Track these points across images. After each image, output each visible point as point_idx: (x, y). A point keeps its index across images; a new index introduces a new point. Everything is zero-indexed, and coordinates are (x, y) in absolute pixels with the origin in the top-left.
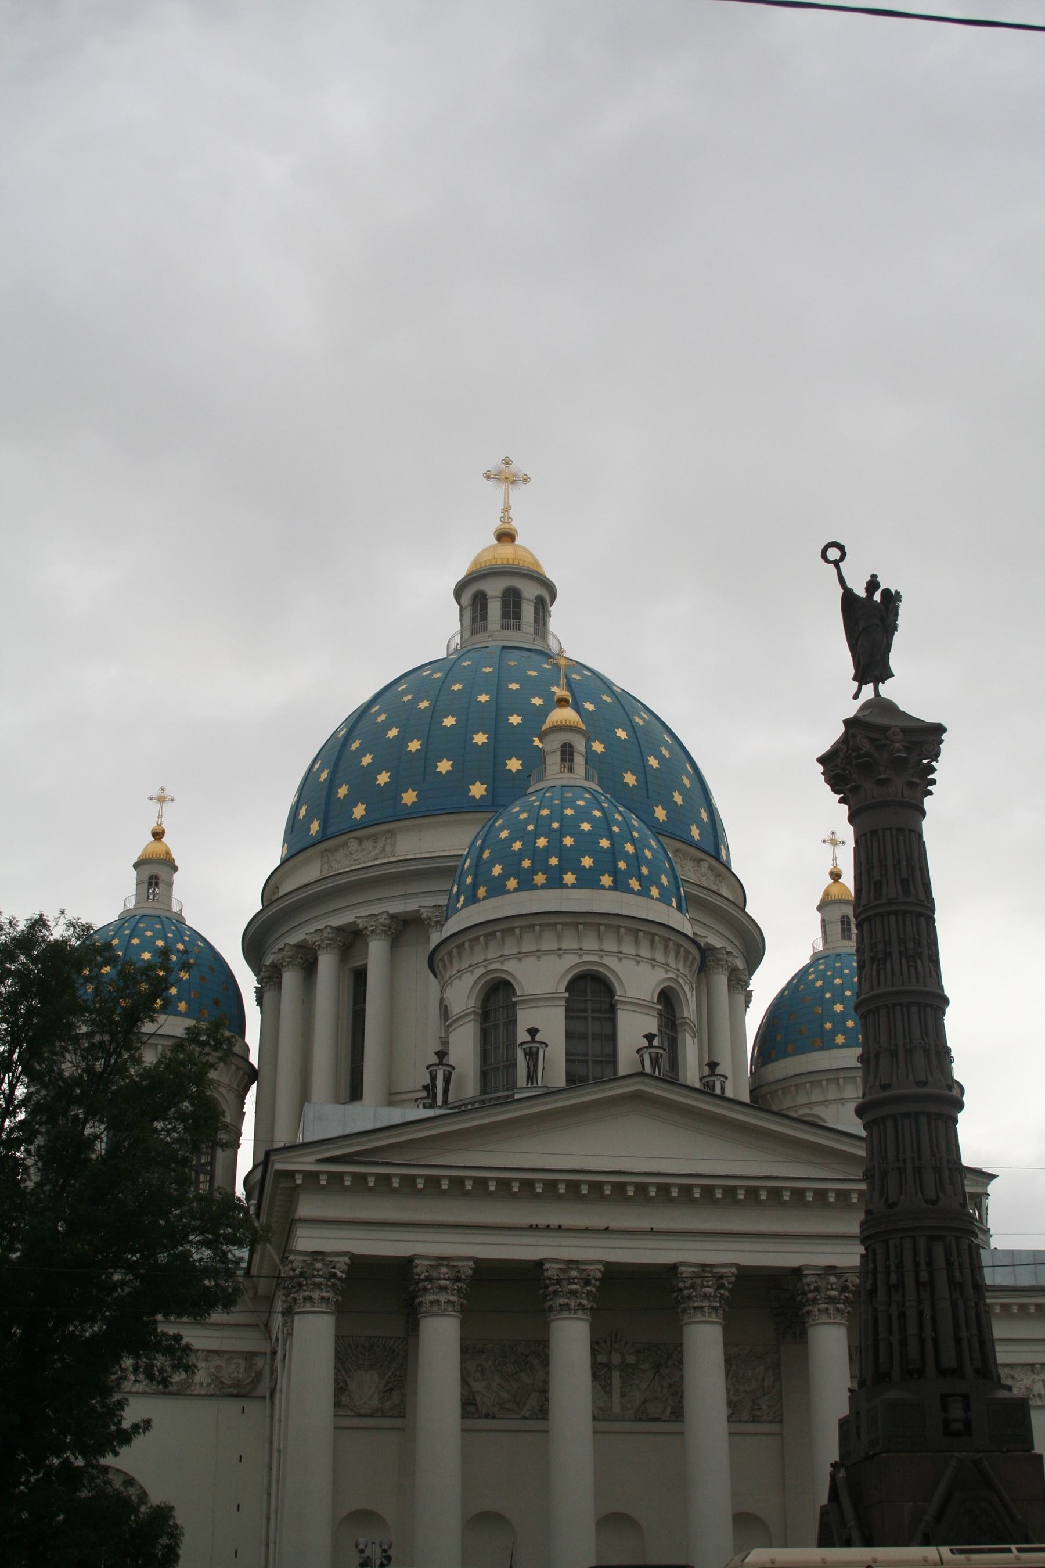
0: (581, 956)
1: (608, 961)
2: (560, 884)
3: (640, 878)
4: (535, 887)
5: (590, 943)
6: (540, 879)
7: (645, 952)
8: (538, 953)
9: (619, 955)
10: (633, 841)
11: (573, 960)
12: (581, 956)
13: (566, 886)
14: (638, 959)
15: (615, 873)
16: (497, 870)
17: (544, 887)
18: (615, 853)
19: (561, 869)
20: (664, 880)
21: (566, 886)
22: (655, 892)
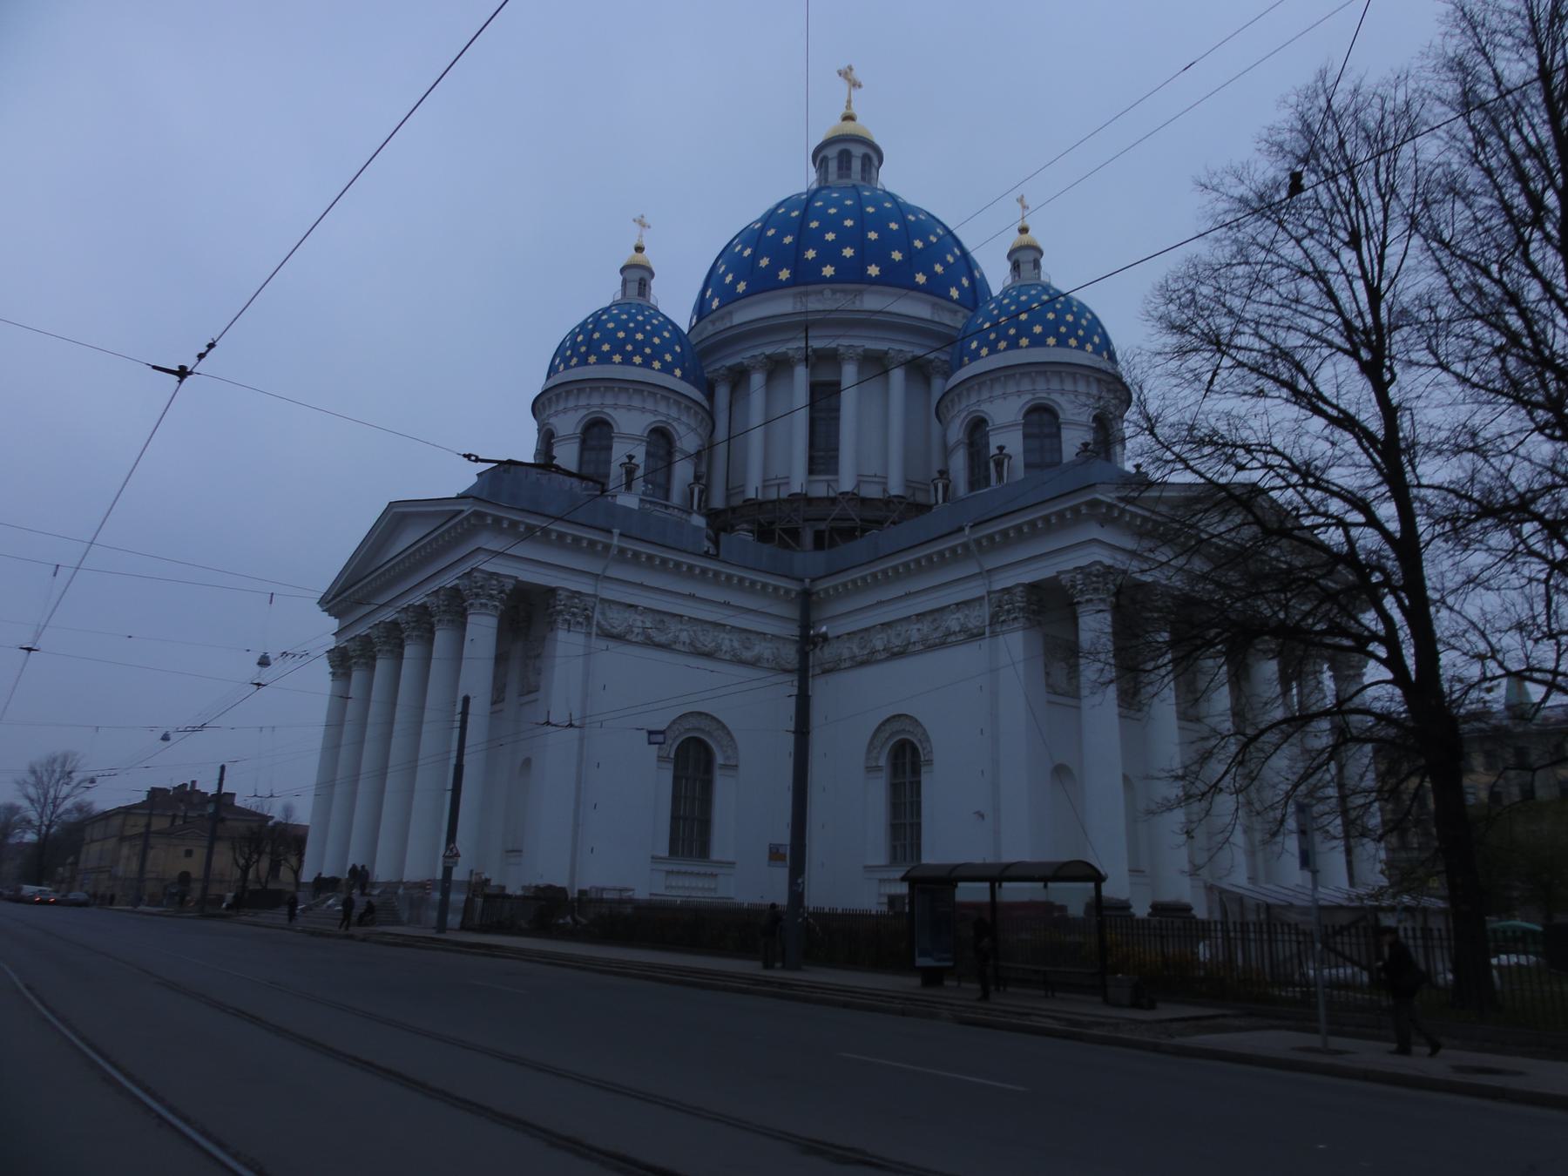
0: (588, 409)
1: (606, 410)
2: (587, 363)
3: (642, 355)
4: (571, 367)
5: (596, 400)
6: (574, 361)
7: (637, 402)
8: (565, 410)
9: (615, 407)
10: (644, 332)
11: (585, 412)
12: (588, 409)
13: (590, 364)
14: (629, 408)
15: (623, 352)
16: (557, 361)
17: (576, 365)
18: (625, 341)
19: (588, 354)
20: (668, 358)
21: (590, 364)
22: (657, 365)
